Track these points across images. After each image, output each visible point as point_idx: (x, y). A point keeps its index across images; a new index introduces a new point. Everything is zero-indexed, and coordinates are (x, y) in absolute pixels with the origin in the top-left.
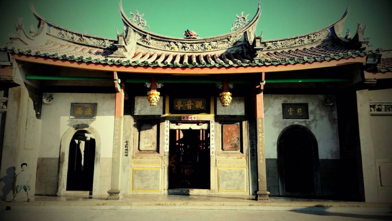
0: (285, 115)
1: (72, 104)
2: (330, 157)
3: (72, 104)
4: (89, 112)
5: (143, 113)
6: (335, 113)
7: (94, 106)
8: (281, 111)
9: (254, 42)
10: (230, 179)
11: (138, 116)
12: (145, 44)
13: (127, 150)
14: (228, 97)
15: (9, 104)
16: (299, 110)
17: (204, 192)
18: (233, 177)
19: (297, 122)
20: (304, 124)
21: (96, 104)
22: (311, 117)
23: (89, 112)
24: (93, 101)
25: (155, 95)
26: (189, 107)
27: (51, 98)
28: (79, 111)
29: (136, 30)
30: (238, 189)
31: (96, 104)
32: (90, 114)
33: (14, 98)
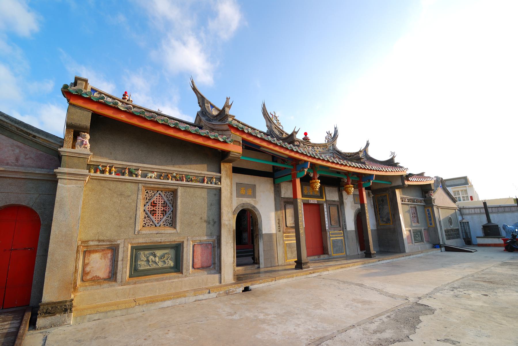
4: (250, 192)
5: (287, 196)
7: (253, 187)
11: (284, 198)
13: (279, 226)
15: (222, 180)
17: (326, 256)
32: (251, 194)
33: (227, 175)
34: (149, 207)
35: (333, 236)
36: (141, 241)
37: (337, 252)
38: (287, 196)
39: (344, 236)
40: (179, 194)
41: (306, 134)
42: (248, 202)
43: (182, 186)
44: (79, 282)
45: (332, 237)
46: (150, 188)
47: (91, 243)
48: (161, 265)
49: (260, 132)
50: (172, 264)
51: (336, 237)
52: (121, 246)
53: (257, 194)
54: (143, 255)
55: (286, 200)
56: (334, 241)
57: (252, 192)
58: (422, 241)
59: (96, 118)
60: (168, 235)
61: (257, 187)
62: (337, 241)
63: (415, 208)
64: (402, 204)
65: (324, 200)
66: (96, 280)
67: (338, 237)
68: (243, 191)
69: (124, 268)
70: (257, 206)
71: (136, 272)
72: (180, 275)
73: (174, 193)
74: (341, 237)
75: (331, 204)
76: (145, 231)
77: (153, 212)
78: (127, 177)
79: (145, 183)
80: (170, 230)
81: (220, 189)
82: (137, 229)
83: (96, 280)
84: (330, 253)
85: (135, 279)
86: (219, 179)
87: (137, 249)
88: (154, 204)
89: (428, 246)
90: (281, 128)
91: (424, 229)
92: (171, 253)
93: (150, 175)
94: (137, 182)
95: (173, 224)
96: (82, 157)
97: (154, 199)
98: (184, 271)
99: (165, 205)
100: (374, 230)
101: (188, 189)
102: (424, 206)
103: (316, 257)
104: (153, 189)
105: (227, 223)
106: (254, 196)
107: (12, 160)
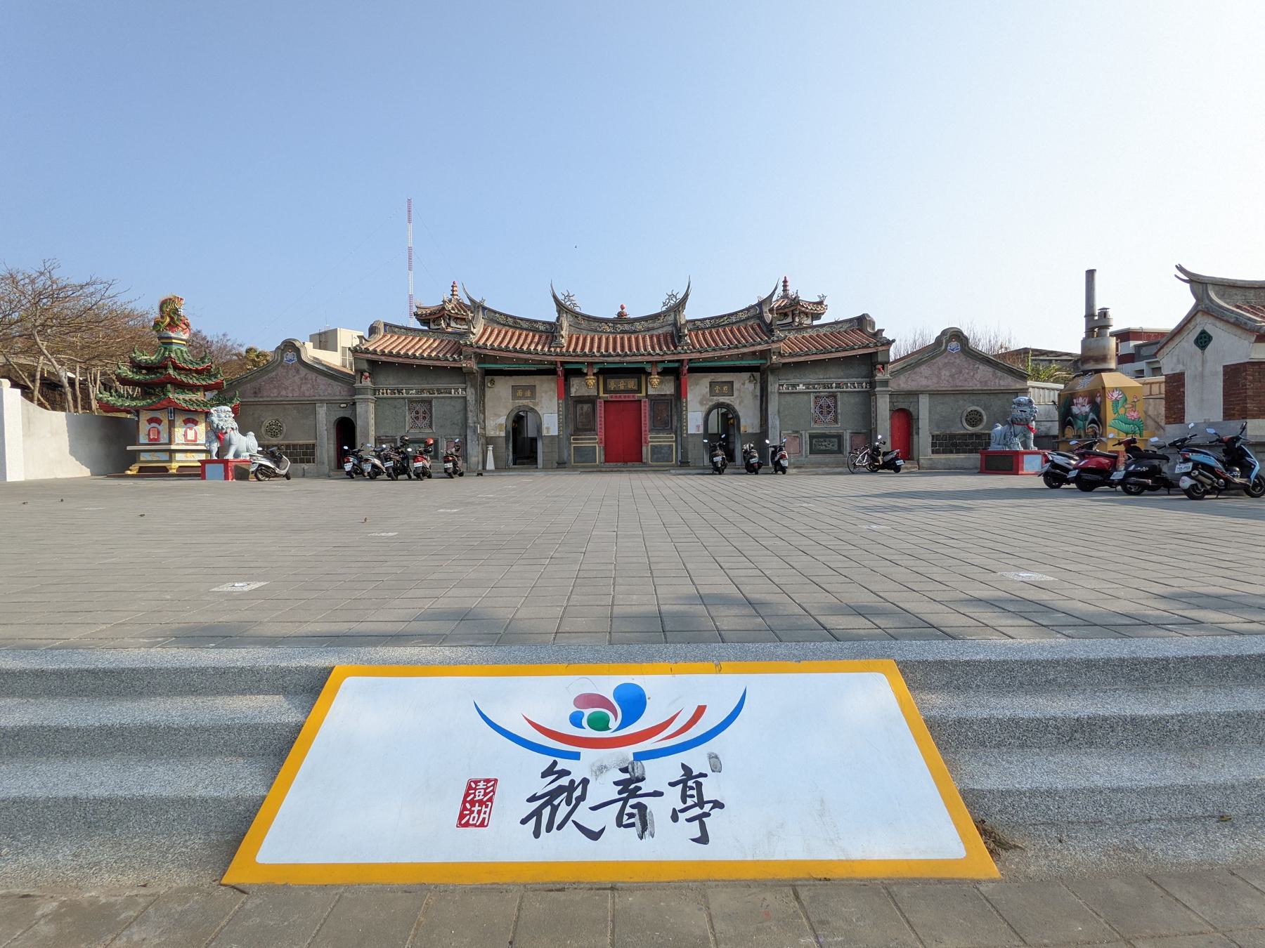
0: (712, 393)
4: (529, 393)
14: (655, 379)
17: (636, 464)
19: (722, 399)
22: (736, 393)
25: (591, 380)
27: (492, 382)
28: (520, 393)
34: (414, 414)
41: (622, 308)
46: (411, 401)
49: (544, 323)
63: (835, 397)
64: (780, 393)
65: (644, 394)
73: (429, 402)
75: (656, 401)
77: (417, 418)
81: (465, 398)
86: (465, 389)
88: (417, 413)
90: (577, 310)
91: (854, 434)
95: (431, 426)
96: (365, 388)
99: (424, 412)
106: (533, 396)
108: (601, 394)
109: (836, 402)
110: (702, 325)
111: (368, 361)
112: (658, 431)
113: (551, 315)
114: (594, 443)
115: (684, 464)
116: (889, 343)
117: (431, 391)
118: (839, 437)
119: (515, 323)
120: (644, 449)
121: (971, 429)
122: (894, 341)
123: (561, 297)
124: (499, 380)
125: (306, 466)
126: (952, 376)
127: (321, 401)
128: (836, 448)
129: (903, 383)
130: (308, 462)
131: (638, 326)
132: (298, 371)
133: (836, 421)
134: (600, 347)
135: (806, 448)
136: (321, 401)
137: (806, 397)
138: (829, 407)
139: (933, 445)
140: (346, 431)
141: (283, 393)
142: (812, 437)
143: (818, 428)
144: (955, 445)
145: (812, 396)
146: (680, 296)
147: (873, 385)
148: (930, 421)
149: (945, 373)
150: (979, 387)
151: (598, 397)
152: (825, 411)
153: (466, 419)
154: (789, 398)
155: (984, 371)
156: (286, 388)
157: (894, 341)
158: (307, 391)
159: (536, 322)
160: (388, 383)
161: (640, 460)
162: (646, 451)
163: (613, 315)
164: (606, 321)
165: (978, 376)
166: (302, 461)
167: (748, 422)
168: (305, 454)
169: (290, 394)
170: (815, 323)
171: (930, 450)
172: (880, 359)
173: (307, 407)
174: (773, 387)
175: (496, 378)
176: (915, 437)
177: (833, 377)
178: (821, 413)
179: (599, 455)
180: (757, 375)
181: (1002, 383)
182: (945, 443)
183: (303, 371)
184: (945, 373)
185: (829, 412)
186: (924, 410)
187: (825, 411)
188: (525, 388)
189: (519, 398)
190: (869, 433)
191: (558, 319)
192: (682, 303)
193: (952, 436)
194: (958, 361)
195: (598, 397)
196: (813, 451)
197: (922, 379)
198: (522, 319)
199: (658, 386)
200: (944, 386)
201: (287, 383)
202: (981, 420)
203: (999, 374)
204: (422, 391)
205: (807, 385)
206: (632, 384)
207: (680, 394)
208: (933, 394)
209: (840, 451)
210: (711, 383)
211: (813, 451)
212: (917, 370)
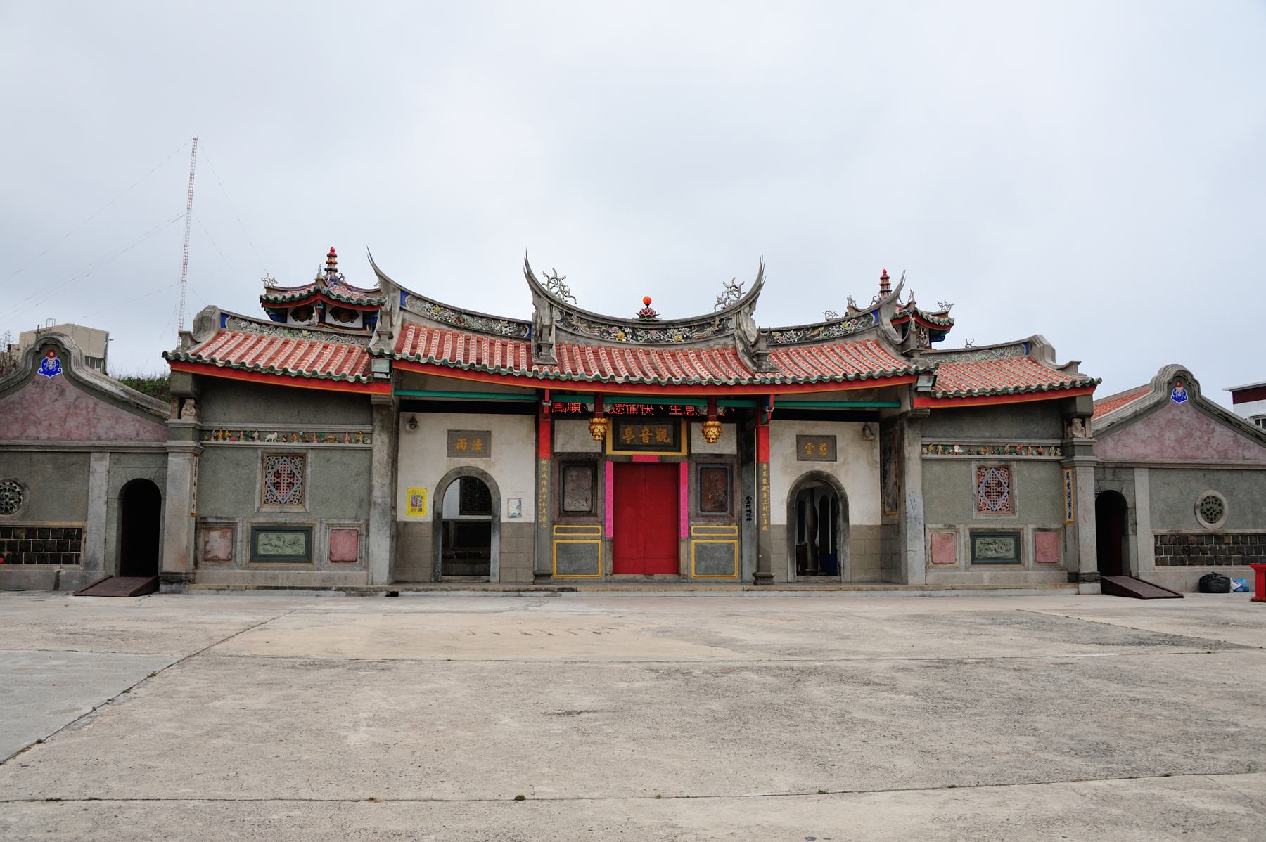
1: (449, 431)
2: (866, 522)
3: (449, 431)
4: (478, 445)
5: (569, 449)
6: (877, 452)
7: (486, 436)
8: (794, 448)
9: (757, 342)
10: (712, 558)
11: (561, 454)
12: (570, 330)
15: (376, 436)
16: (823, 446)
18: (717, 555)
19: (818, 466)
20: (829, 471)
21: (489, 433)
23: (478, 445)
24: (484, 428)
26: (646, 440)
27: (413, 423)
28: (462, 444)
29: (553, 302)
30: (725, 573)
31: (489, 433)
34: (271, 479)
35: (700, 535)
36: (261, 520)
37: (707, 571)
38: (569, 450)
39: (740, 537)
40: (309, 460)
42: (472, 464)
43: (313, 449)
44: (200, 559)
45: (698, 538)
47: (210, 520)
48: (288, 551)
50: (302, 551)
51: (712, 538)
52: (240, 524)
53: (494, 449)
54: (262, 537)
55: (565, 457)
56: (701, 549)
57: (483, 442)
58: (1017, 560)
59: (196, 377)
60: (295, 514)
61: (494, 434)
62: (714, 548)
64: (924, 460)
65: (684, 452)
66: (216, 560)
67: (719, 538)
68: (462, 444)
69: (243, 552)
70: (493, 472)
71: (256, 557)
72: (310, 565)
73: (302, 457)
74: (730, 538)
76: (266, 509)
78: (242, 442)
79: (265, 448)
80: (297, 509)
82: (257, 505)
83: (216, 560)
84: (683, 570)
85: (255, 565)
87: (257, 530)
88: (278, 475)
89: (1034, 576)
90: (570, 302)
92: (302, 538)
93: (269, 437)
94: (255, 448)
95: (301, 501)
97: (278, 467)
98: (316, 562)
99: (291, 475)
100: (871, 528)
101: (322, 453)
102: (1058, 461)
103: (639, 577)
104: (276, 455)
105: (379, 501)
106: (485, 452)
107: (134, 435)
108: (609, 451)
109: (1010, 476)
110: (784, 339)
111: (195, 376)
112: (709, 519)
113: (522, 308)
114: (593, 538)
115: (762, 579)
116: (1093, 385)
117: (305, 437)
118: (1016, 536)
119: (460, 320)
120: (683, 548)
121: (1210, 527)
122: (1099, 381)
123: (542, 280)
124: (425, 419)
125: (63, 570)
126: (1179, 441)
127: (101, 449)
128: (1012, 554)
129: (1113, 450)
130: (68, 561)
131: (676, 335)
132: (62, 392)
133: (1010, 509)
134: (624, 365)
135: (964, 554)
136: (101, 449)
137: (963, 467)
138: (999, 484)
139: (1157, 551)
140: (140, 506)
141: (31, 431)
142: (975, 535)
143: (986, 521)
144: (1186, 551)
145: (974, 466)
146: (747, 289)
147: (1067, 448)
148: (1152, 512)
149: (1170, 436)
150: (1216, 460)
151: (603, 454)
152: (994, 489)
153: (370, 489)
154: (937, 469)
155: (1222, 435)
156: (37, 423)
157: (1099, 381)
158: (76, 431)
159: (497, 320)
160: (230, 417)
161: (675, 569)
162: (688, 552)
163: (630, 312)
164: (621, 324)
165: (1214, 443)
166: (55, 561)
167: (863, 508)
168: (62, 546)
169: (39, 434)
170: (937, 346)
171: (1152, 557)
172: (1080, 407)
173: (73, 457)
174: (913, 451)
175: (422, 417)
176: (1131, 538)
177: (1005, 433)
178: (988, 494)
179: (604, 561)
180: (876, 426)
181: (1247, 454)
182: (1175, 549)
183: (72, 392)
184: (1170, 436)
185: (1000, 494)
186: (1143, 497)
187: (994, 489)
188: (471, 436)
189: (460, 453)
190: (1065, 531)
191: (536, 315)
192: (751, 300)
193: (1183, 538)
194: (1185, 417)
195: (603, 454)
196: (975, 560)
197: (1136, 445)
198: (472, 315)
199: (715, 440)
200: (1169, 457)
201: (40, 414)
202: (1221, 512)
203: (1243, 440)
204: (287, 436)
205: (968, 448)
206: (663, 435)
207: (749, 454)
208: (1154, 468)
209: (1017, 560)
210: (801, 439)
211: (975, 560)
212: (1130, 429)
